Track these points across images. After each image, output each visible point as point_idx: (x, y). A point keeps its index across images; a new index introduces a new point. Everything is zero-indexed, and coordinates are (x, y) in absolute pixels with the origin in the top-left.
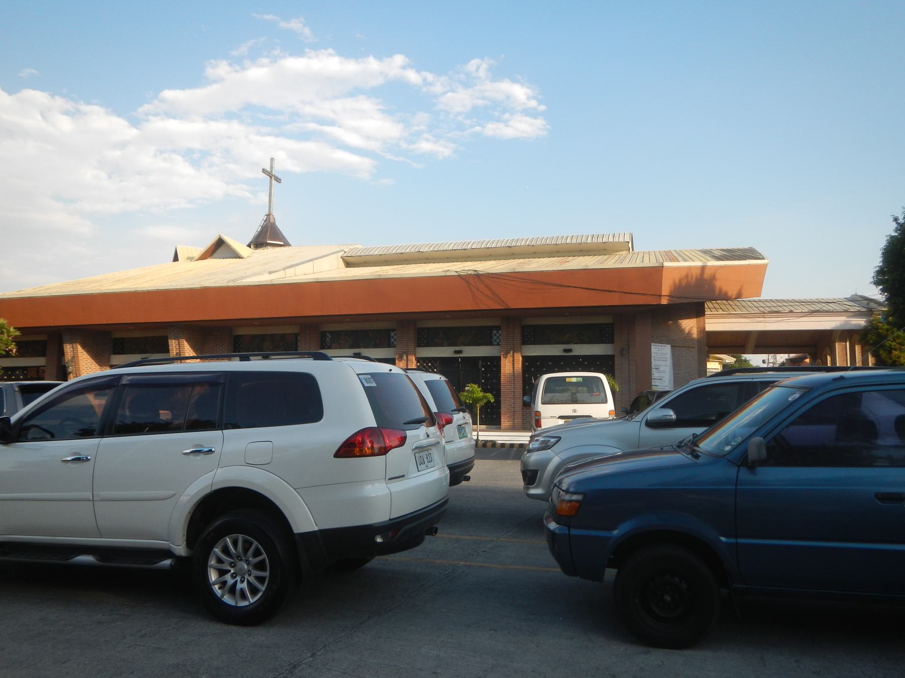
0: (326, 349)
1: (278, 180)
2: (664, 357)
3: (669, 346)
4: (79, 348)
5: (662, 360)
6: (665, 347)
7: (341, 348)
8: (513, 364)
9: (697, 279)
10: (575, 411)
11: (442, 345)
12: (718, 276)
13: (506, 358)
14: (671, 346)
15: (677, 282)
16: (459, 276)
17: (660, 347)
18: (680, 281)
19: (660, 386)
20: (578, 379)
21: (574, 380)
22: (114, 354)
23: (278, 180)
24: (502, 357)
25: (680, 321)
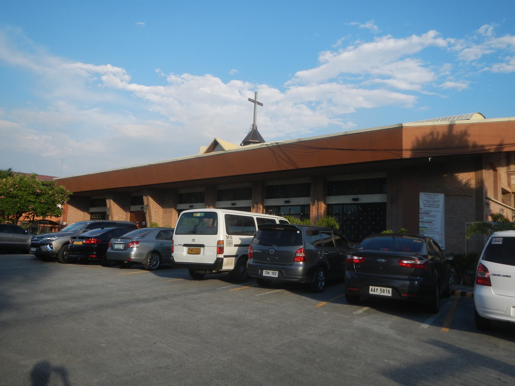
0: (220, 201)
1: (261, 104)
4: (112, 202)
5: (433, 207)
6: (438, 195)
7: (227, 201)
8: (318, 210)
9: (444, 135)
10: (194, 240)
11: (280, 197)
12: (470, 132)
13: (313, 205)
14: (445, 195)
15: (420, 139)
16: (268, 147)
17: (432, 196)
18: (424, 138)
19: (429, 228)
20: (202, 214)
22: (133, 205)
23: (261, 104)
24: (311, 205)
25: (457, 174)
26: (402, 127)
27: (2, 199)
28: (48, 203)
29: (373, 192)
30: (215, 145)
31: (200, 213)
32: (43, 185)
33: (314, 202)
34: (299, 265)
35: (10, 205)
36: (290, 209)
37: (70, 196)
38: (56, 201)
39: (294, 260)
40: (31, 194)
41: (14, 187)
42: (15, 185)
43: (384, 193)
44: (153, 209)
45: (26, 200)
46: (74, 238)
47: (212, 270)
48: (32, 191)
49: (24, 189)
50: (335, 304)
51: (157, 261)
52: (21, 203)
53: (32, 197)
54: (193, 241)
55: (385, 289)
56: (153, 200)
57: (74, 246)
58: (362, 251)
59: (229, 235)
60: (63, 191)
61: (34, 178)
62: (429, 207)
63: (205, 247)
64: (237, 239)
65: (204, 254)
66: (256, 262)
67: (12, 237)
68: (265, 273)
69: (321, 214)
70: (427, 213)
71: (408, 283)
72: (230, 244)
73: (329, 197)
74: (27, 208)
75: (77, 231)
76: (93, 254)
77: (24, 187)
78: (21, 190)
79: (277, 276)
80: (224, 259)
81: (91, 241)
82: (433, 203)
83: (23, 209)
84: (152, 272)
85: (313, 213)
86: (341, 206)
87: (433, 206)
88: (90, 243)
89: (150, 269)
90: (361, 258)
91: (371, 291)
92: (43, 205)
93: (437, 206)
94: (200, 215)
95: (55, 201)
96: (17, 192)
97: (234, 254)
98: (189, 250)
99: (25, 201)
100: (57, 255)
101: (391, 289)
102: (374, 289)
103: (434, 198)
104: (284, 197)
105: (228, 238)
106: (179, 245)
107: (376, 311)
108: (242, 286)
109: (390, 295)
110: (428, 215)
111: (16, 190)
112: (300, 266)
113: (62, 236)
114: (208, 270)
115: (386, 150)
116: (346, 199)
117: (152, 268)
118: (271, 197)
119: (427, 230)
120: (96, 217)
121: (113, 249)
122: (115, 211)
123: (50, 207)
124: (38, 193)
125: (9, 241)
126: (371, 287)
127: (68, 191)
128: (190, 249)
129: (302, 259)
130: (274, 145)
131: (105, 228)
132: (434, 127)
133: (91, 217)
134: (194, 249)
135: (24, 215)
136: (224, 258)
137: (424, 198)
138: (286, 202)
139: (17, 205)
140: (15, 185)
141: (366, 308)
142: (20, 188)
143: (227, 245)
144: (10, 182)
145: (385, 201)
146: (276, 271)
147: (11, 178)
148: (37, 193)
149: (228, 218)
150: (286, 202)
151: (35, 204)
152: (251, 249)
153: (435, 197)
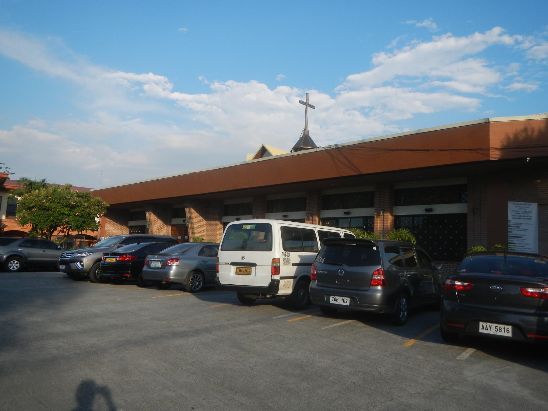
0: (270, 213)
1: (313, 107)
2: (526, 215)
3: (537, 204)
4: (152, 214)
5: (524, 219)
6: (530, 205)
8: (384, 222)
9: (540, 132)
10: (243, 258)
11: (338, 208)
13: (378, 217)
14: (539, 205)
15: (512, 136)
16: (326, 150)
18: (516, 136)
20: (253, 226)
21: (249, 227)
23: (313, 107)
24: (375, 216)
26: (489, 122)
27: (34, 212)
28: (83, 215)
29: (450, 201)
30: (263, 151)
31: (250, 225)
32: (78, 196)
33: (379, 213)
34: (377, 291)
35: (43, 218)
36: (350, 222)
37: (107, 208)
38: (92, 214)
39: (371, 285)
40: (65, 206)
41: (47, 199)
42: (47, 197)
43: (464, 203)
44: (196, 222)
45: (59, 212)
46: (106, 254)
47: (266, 295)
48: (67, 203)
49: (58, 201)
50: (428, 344)
51: (199, 282)
52: (54, 216)
53: (66, 209)
54: (243, 259)
55: (502, 326)
56: (195, 212)
57: (106, 264)
58: (465, 274)
59: (286, 252)
60: (100, 203)
61: (68, 189)
62: (518, 218)
63: (257, 266)
64: (295, 257)
65: (256, 275)
66: (320, 286)
67: (44, 253)
68: (333, 300)
69: (388, 227)
70: (517, 226)
71: (534, 319)
72: (287, 262)
73: (398, 207)
74: (61, 222)
75: (111, 247)
76: (128, 273)
77: (57, 199)
78: (54, 202)
79: (348, 304)
80: (281, 281)
81: (125, 258)
82: (524, 214)
83: (56, 223)
84: (194, 295)
85: (378, 225)
86: (411, 218)
87: (523, 217)
88: (124, 260)
89: (191, 291)
90: (466, 284)
91: (482, 329)
92: (78, 218)
93: (529, 218)
94: (251, 227)
95: (90, 213)
96: (50, 204)
97: (293, 275)
98: (237, 270)
99: (58, 214)
100: (88, 274)
101: (510, 328)
102: (487, 327)
103: (525, 208)
104: (343, 208)
105: (285, 255)
106: (226, 263)
107: (487, 355)
108: (303, 315)
109: (510, 335)
110: (518, 229)
111: (50, 202)
112: (378, 292)
113: (94, 252)
114: (261, 295)
115: (471, 150)
116: (417, 210)
117: (194, 290)
118: (328, 208)
119: (516, 246)
120: (135, 231)
121: (149, 267)
122: (155, 224)
123: (85, 221)
124: (73, 205)
125: (41, 257)
126: (481, 324)
127: (105, 202)
128: (238, 269)
129: (381, 283)
130: (333, 147)
131: (141, 243)
132: (528, 122)
133: (130, 231)
134: (244, 269)
135: (58, 229)
136: (280, 280)
137: (512, 207)
138: (345, 213)
139: (50, 218)
140: (47, 197)
141: (470, 351)
142: (53, 200)
143: (284, 264)
144: (43, 194)
145: (465, 211)
146: (346, 298)
147: (44, 189)
148: (71, 205)
149: (285, 231)
150: (345, 213)
151: (69, 217)
152: (315, 269)
153: (527, 207)
